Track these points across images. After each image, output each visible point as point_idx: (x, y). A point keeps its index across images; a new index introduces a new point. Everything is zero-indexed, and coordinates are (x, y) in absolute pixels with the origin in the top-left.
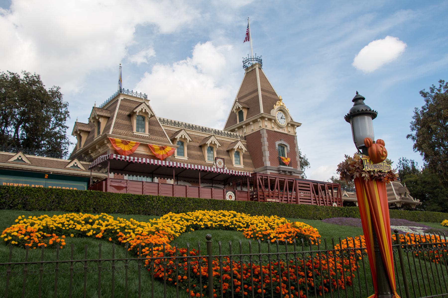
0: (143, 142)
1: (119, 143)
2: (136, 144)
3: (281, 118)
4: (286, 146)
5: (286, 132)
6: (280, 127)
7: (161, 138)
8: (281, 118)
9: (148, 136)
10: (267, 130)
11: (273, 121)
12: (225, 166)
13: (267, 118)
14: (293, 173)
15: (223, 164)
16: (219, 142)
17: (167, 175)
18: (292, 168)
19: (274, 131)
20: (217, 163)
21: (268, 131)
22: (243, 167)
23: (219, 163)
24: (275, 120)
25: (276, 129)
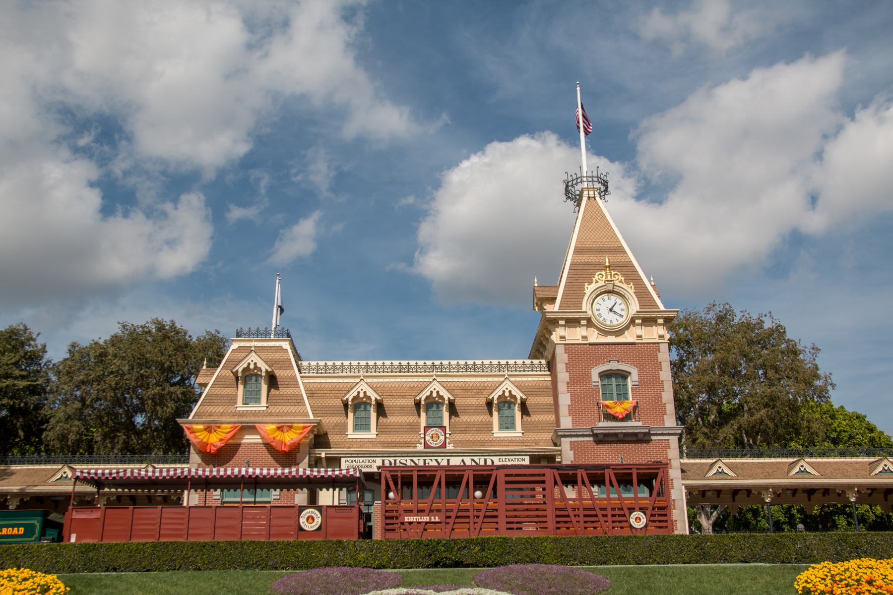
0: (247, 423)
1: (200, 431)
2: (231, 428)
3: (611, 310)
4: (630, 373)
5: (629, 337)
6: (605, 332)
7: (293, 409)
8: (611, 310)
9: (265, 408)
10: (565, 344)
11: (584, 322)
12: (448, 441)
13: (562, 319)
16: (448, 390)
17: (231, 484)
18: (640, 424)
19: (591, 344)
20: (428, 438)
21: (570, 348)
22: (520, 435)
23: (432, 437)
24: (589, 320)
25: (594, 337)
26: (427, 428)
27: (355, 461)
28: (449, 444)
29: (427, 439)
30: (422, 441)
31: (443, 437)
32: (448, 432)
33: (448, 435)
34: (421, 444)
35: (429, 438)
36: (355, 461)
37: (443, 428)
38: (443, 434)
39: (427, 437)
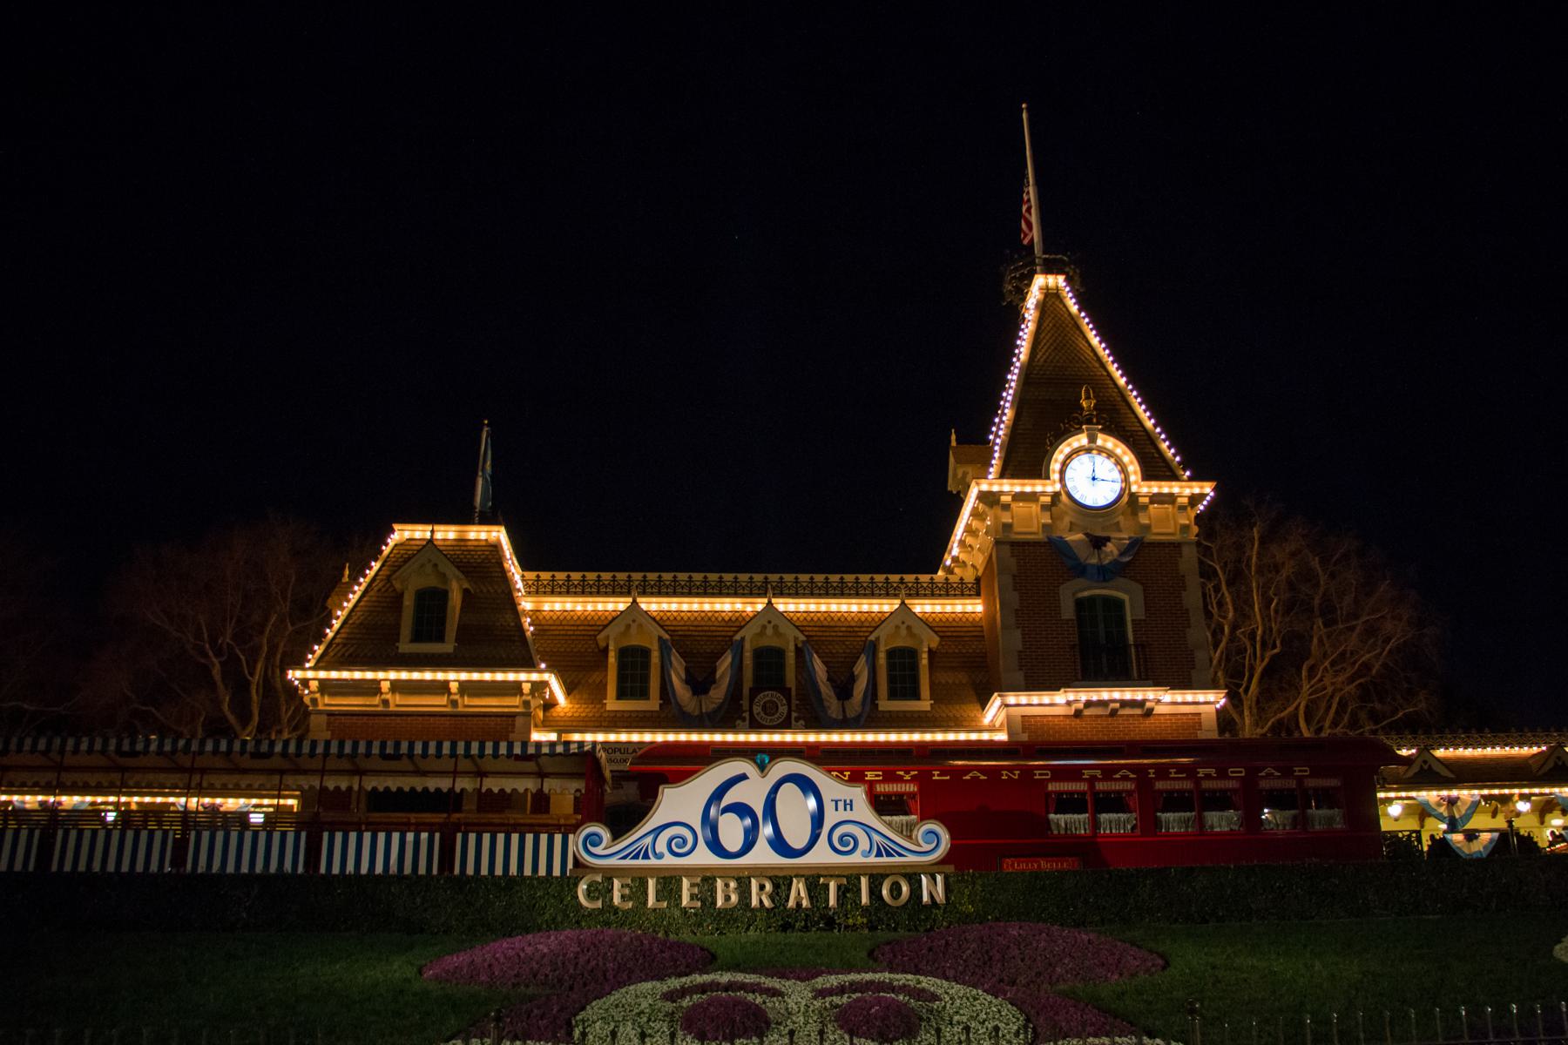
12: (794, 715)
14: (1148, 705)
15: (783, 709)
20: (757, 709)
23: (764, 708)
26: (754, 692)
27: (620, 750)
28: (797, 721)
29: (755, 712)
30: (746, 715)
31: (786, 708)
32: (794, 702)
33: (793, 708)
34: (744, 720)
35: (760, 709)
36: (620, 750)
37: (786, 692)
38: (784, 702)
39: (755, 707)
